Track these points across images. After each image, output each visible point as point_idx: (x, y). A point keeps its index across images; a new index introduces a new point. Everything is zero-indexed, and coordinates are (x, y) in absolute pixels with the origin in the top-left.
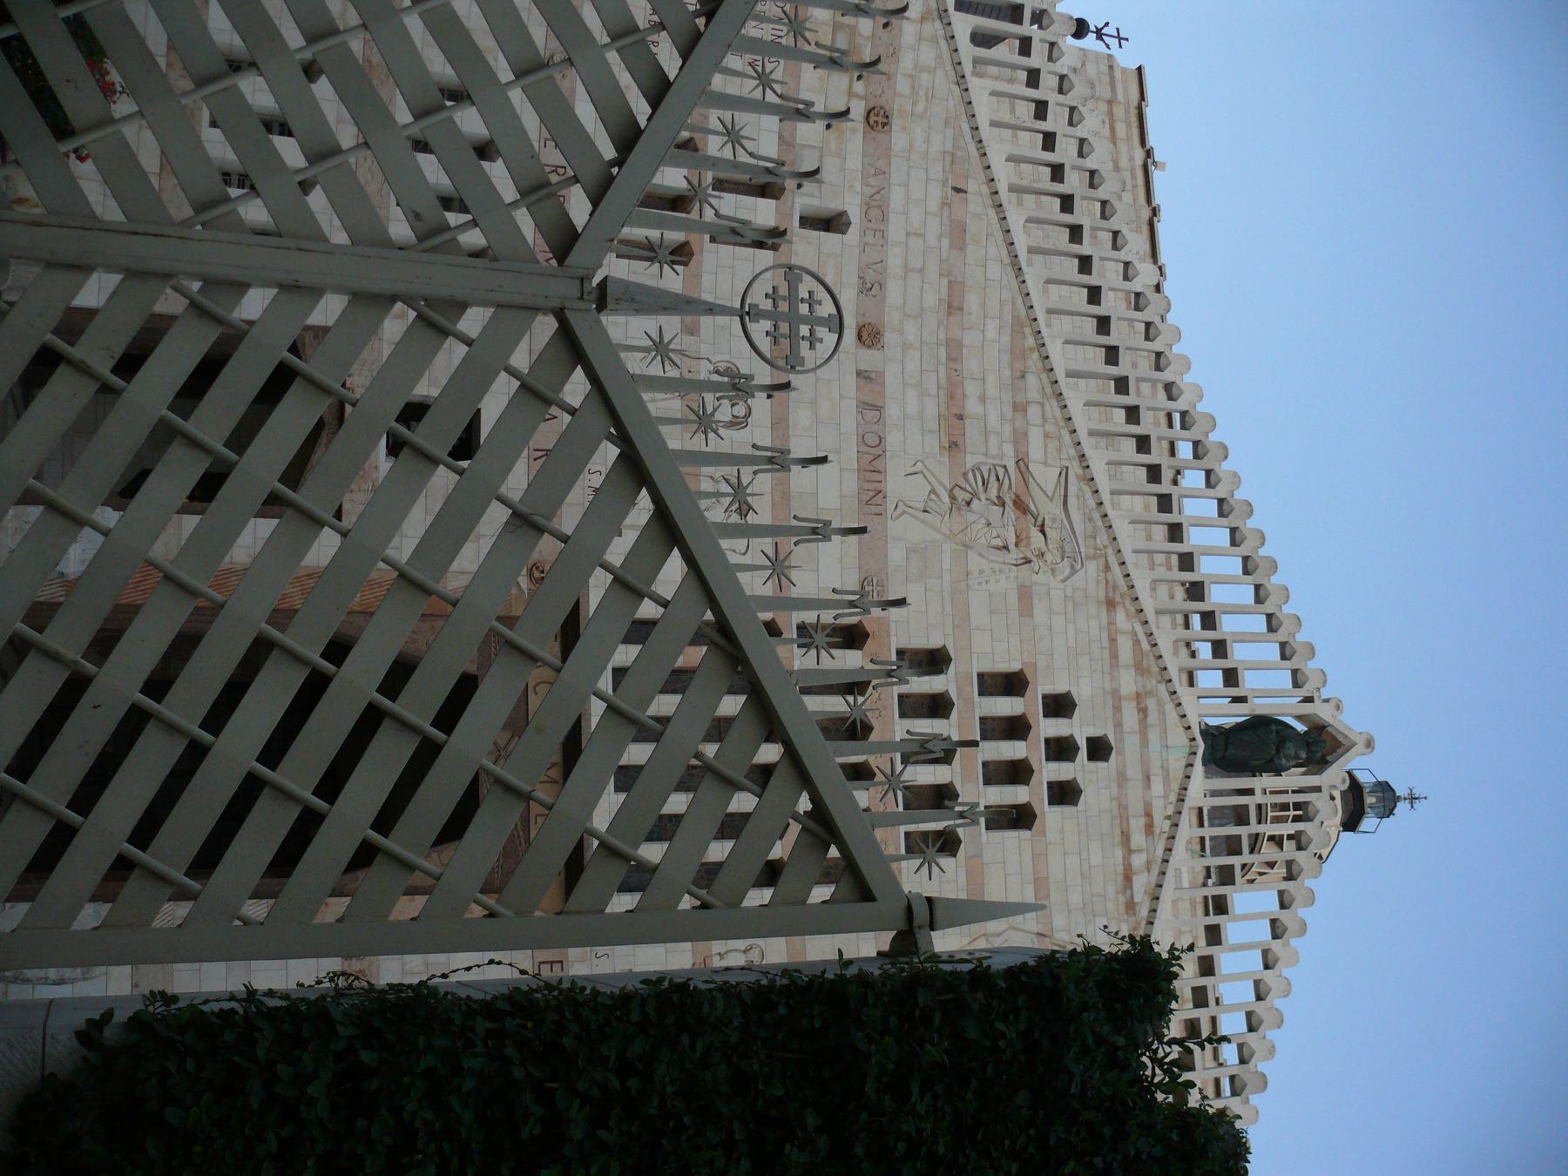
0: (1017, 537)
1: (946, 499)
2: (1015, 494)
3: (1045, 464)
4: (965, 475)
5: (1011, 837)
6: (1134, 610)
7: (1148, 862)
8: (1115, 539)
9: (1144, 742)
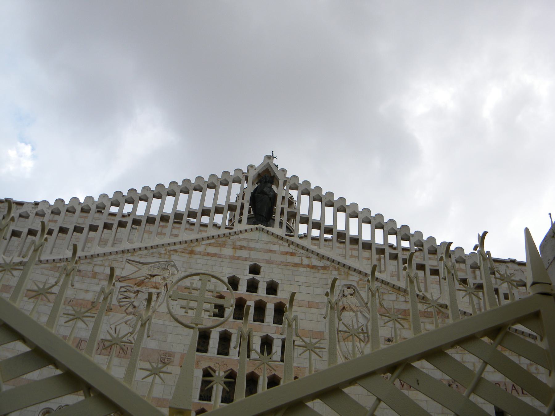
0: (154, 288)
1: (131, 317)
2: (134, 285)
3: (123, 269)
4: (121, 306)
6: (196, 243)
7: (307, 257)
8: (163, 245)
9: (254, 249)
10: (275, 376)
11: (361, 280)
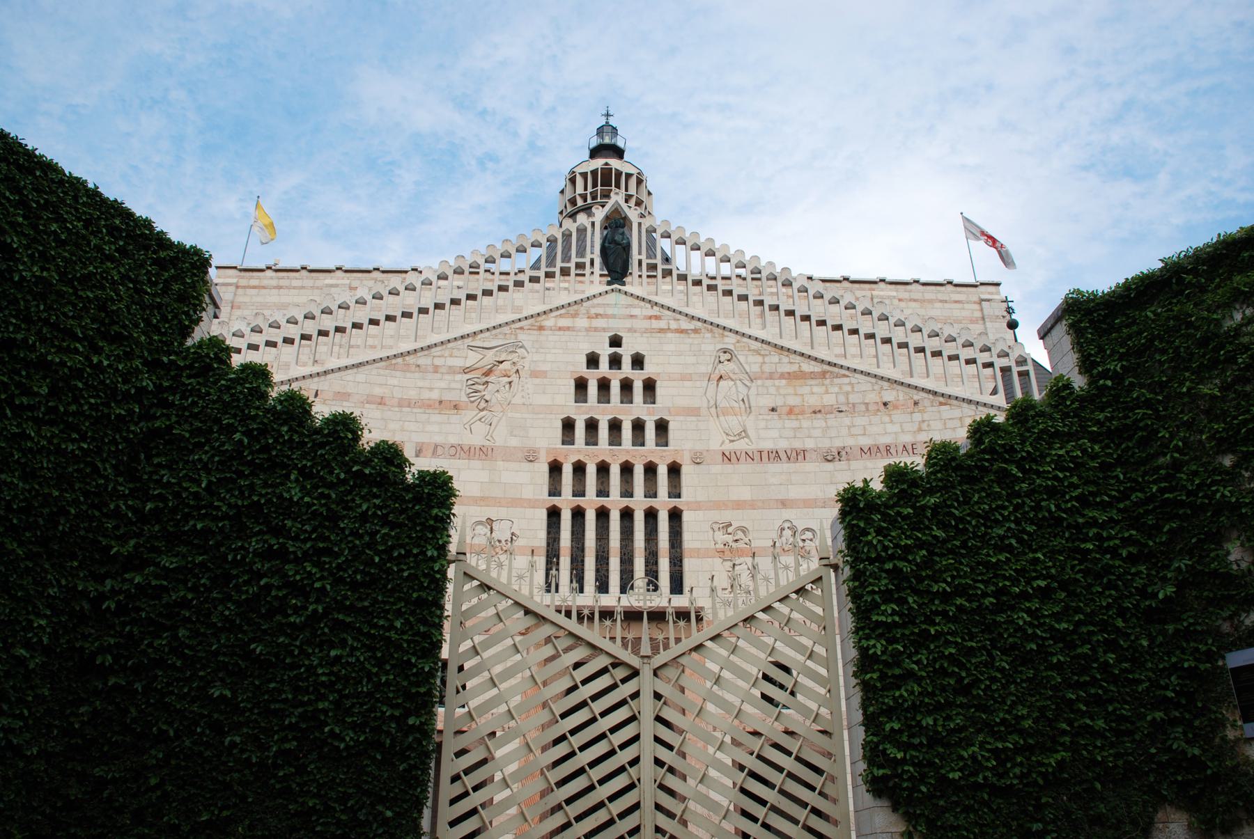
1: (484, 413)
5: (660, 391)
9: (614, 316)
10: (651, 462)
11: (738, 342)
